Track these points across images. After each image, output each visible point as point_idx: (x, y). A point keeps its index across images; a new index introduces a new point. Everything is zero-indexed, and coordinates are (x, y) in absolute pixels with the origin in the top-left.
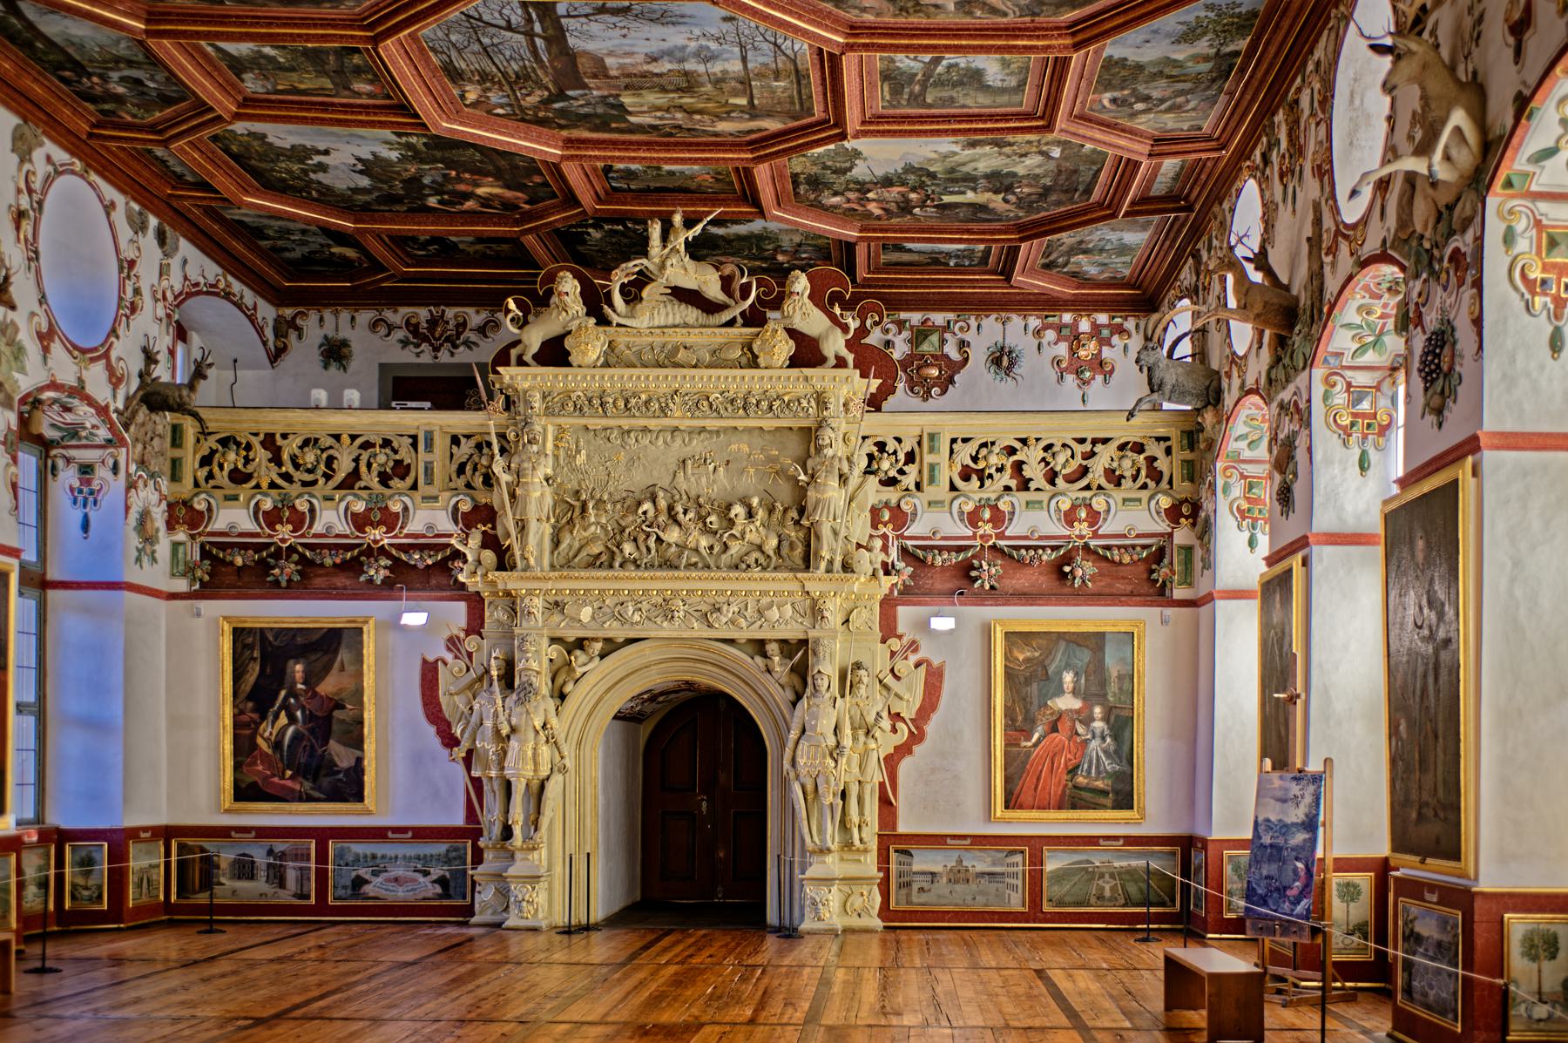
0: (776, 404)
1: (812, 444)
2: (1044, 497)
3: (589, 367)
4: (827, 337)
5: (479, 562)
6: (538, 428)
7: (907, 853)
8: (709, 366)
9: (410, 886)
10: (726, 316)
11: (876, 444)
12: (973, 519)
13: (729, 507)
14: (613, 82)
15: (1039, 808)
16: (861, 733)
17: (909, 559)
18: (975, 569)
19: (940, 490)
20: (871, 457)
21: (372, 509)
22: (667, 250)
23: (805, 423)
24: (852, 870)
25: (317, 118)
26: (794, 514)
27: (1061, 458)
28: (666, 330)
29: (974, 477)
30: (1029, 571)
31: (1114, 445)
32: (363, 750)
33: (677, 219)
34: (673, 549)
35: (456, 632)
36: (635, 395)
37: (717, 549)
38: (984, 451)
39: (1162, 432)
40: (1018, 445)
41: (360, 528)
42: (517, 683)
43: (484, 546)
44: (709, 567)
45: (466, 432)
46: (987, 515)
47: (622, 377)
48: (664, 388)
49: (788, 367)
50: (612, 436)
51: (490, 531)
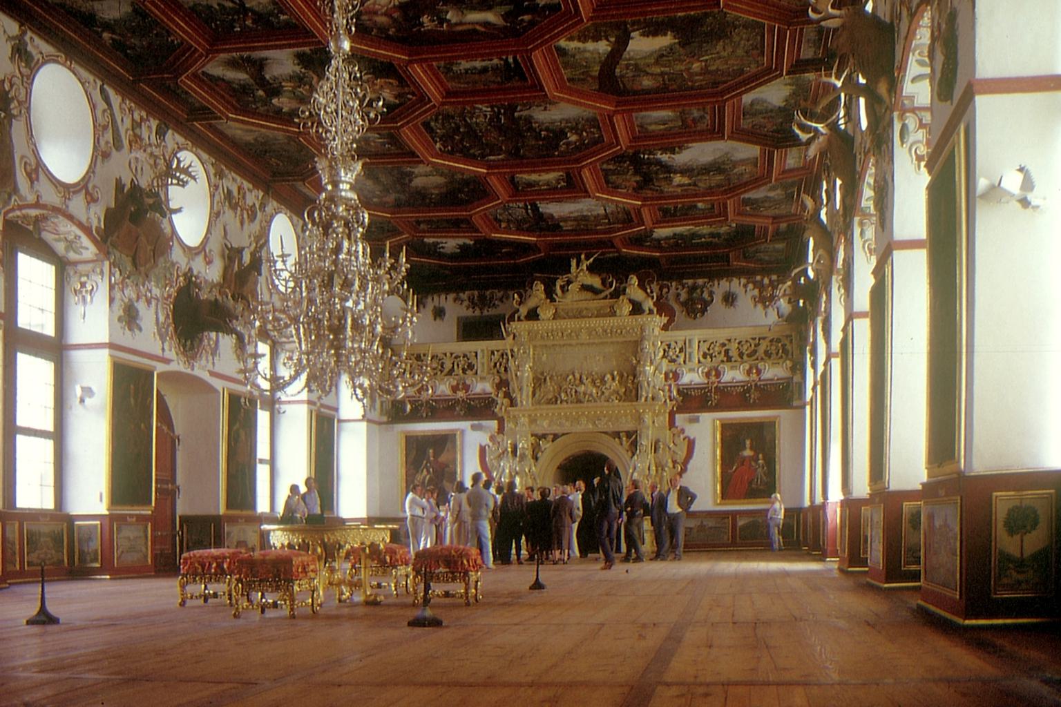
0: (624, 331)
2: (738, 364)
5: (503, 404)
16: (660, 469)
20: (664, 351)
23: (636, 339)
26: (632, 378)
27: (745, 347)
31: (768, 340)
39: (788, 333)
40: (727, 342)
43: (505, 397)
46: (713, 373)
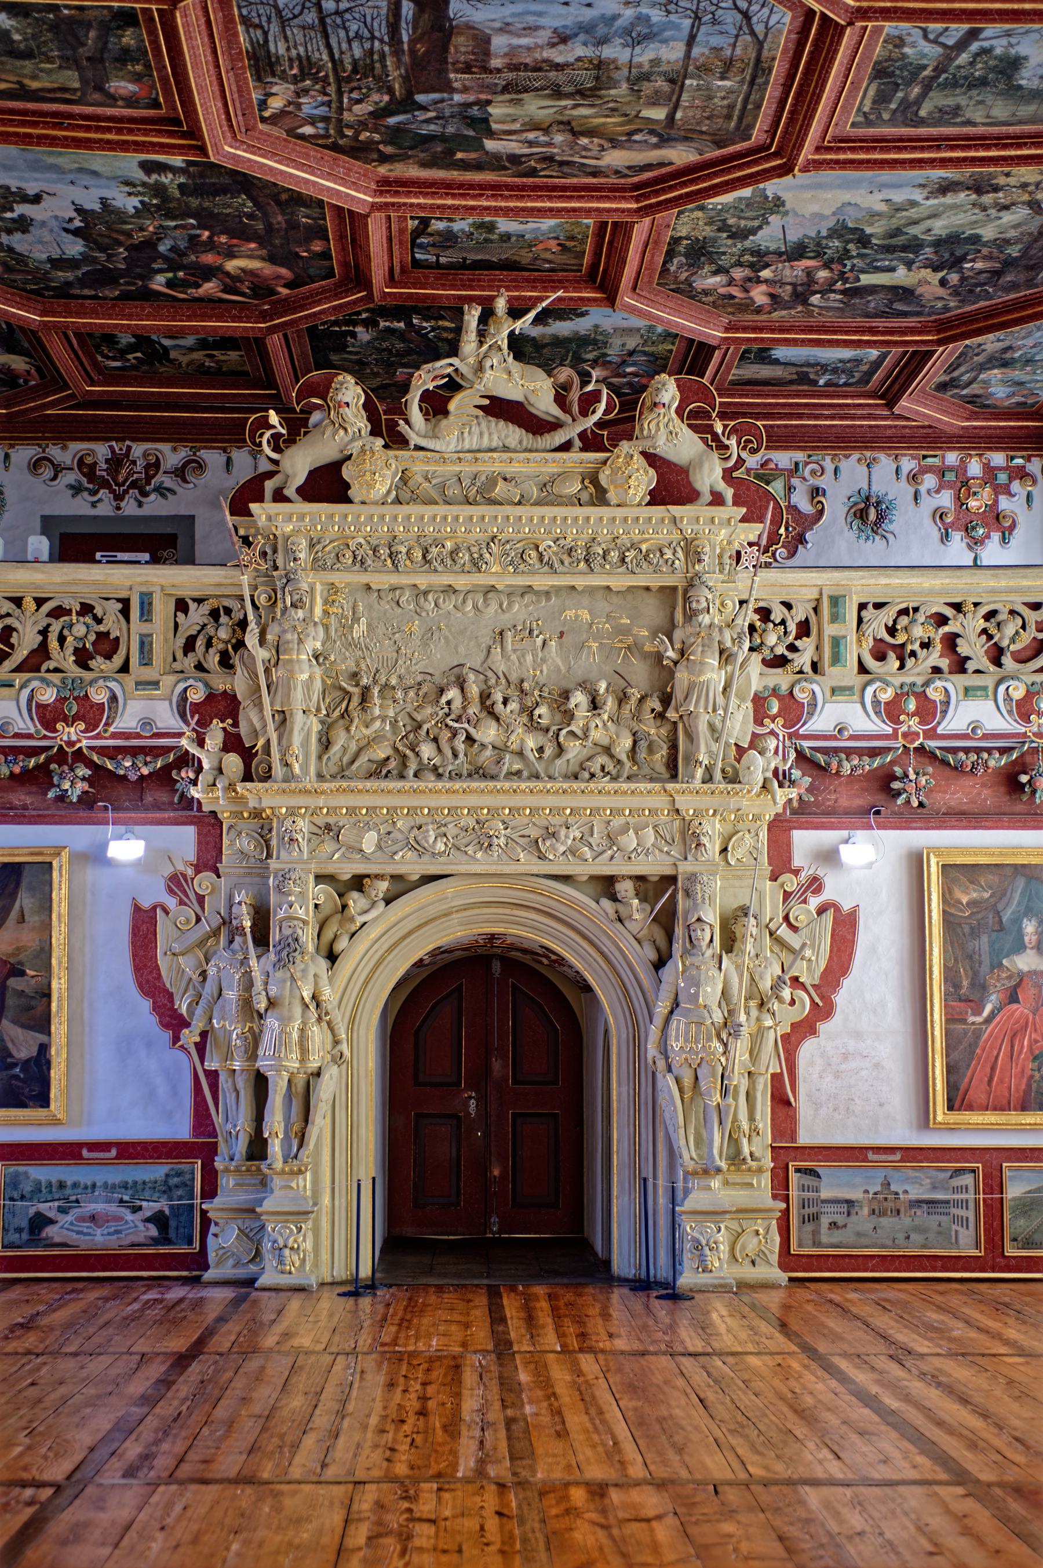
0: (630, 555)
1: (679, 610)
2: (988, 681)
3: (376, 503)
4: (701, 464)
5: (220, 771)
6: (305, 586)
7: (812, 1172)
8: (538, 503)
9: (113, 1227)
10: (559, 438)
11: (757, 611)
12: (892, 711)
13: (566, 695)
14: (489, 79)
15: (995, 1109)
16: (753, 1004)
17: (806, 766)
18: (896, 778)
19: (846, 674)
21: (66, 699)
22: (485, 347)
23: (669, 581)
24: (739, 1197)
25: (46, 137)
28: (479, 455)
29: (892, 655)
30: (967, 782)
32: (49, 1034)
33: (501, 305)
34: (488, 752)
35: (181, 867)
36: (439, 543)
37: (548, 752)
38: (904, 621)
40: (949, 612)
41: (49, 725)
42: (274, 936)
43: (226, 748)
44: (537, 777)
45: (196, 594)
46: (912, 706)
47: (422, 518)
48: (477, 534)
49: (649, 504)
50: (403, 599)
51: (229, 728)
